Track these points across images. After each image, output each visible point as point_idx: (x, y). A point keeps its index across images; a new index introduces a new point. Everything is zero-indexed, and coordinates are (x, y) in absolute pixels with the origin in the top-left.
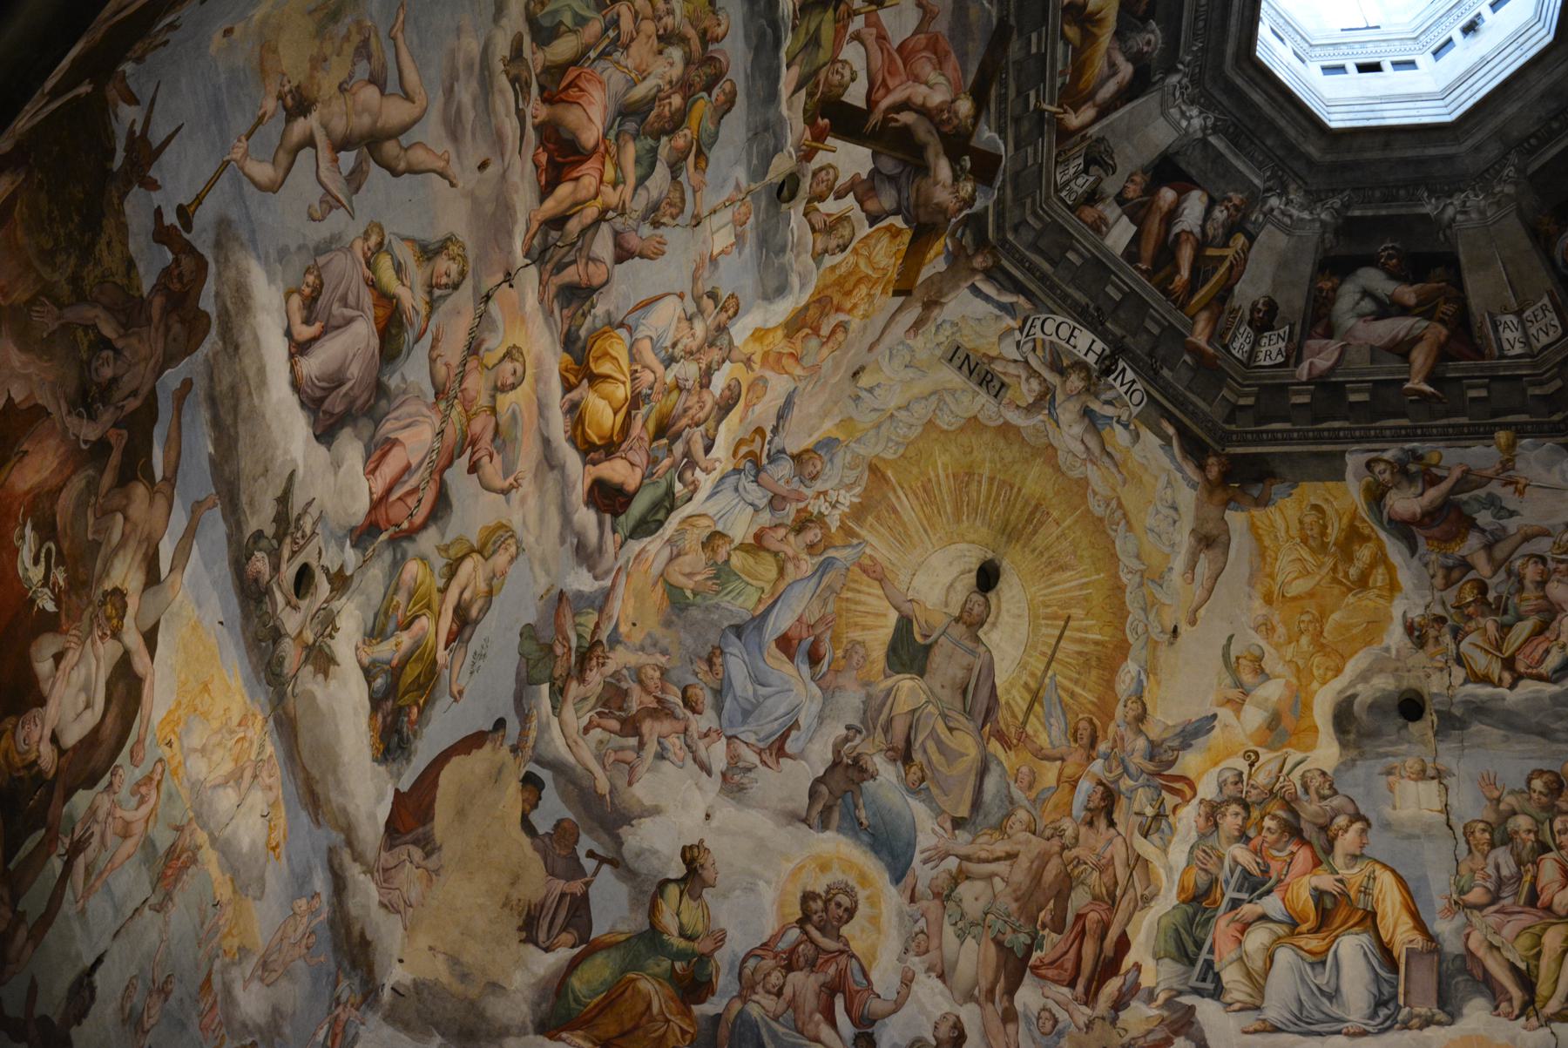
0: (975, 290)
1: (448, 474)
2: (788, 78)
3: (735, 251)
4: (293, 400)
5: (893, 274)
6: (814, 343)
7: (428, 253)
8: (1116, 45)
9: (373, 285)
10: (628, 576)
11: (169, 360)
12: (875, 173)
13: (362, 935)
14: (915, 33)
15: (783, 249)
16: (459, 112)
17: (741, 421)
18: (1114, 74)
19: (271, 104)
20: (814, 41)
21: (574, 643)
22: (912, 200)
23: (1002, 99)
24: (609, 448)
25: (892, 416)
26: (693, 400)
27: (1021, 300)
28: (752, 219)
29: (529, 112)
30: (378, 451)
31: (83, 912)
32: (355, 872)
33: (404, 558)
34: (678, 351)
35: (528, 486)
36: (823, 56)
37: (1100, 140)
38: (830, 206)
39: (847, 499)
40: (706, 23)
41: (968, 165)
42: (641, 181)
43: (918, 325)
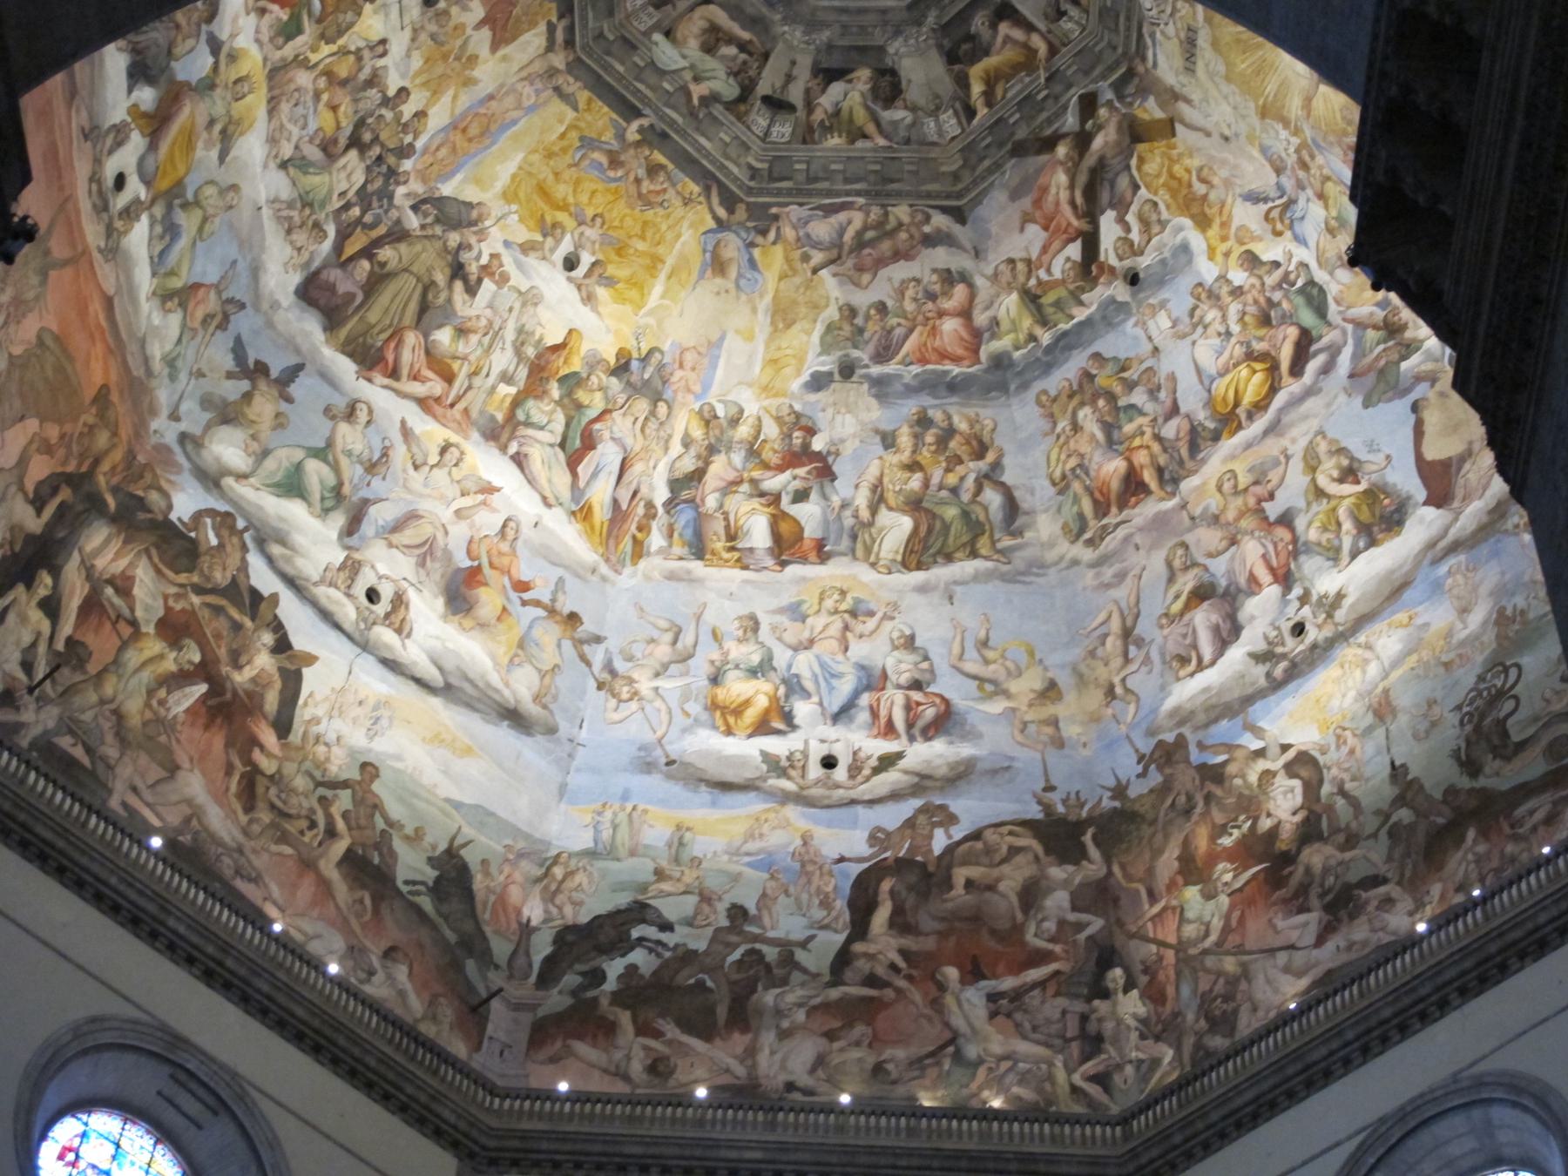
0: (1155, 65)
1: (1272, 519)
2: (1081, 314)
3: (1169, 306)
4: (1220, 662)
5: (1160, 146)
6: (1213, 196)
7: (1171, 579)
8: (994, 49)
9: (1182, 614)
10: (1348, 308)
11: (1187, 761)
12: (1112, 206)
13: (1491, 512)
14: (1035, 222)
15: (1163, 262)
16: (1115, 576)
17: (1260, 239)
18: (1007, 39)
19: (1110, 711)
20: (1058, 304)
21: (1381, 347)
22: (1119, 159)
23: (1049, 121)
24: (1273, 368)
25: (1235, 108)
26: (1249, 298)
27: (1145, 30)
28: (1151, 301)
29: (1114, 521)
30: (1254, 584)
31: (1368, 780)
32: (1453, 533)
33: (1306, 543)
34: (1222, 330)
35: (1284, 442)
36: (1061, 292)
37: (1046, 16)
38: (1135, 236)
39: (1284, 134)
40: (1064, 398)
41: (1090, 122)
42: (1141, 413)
43: (1188, 101)
